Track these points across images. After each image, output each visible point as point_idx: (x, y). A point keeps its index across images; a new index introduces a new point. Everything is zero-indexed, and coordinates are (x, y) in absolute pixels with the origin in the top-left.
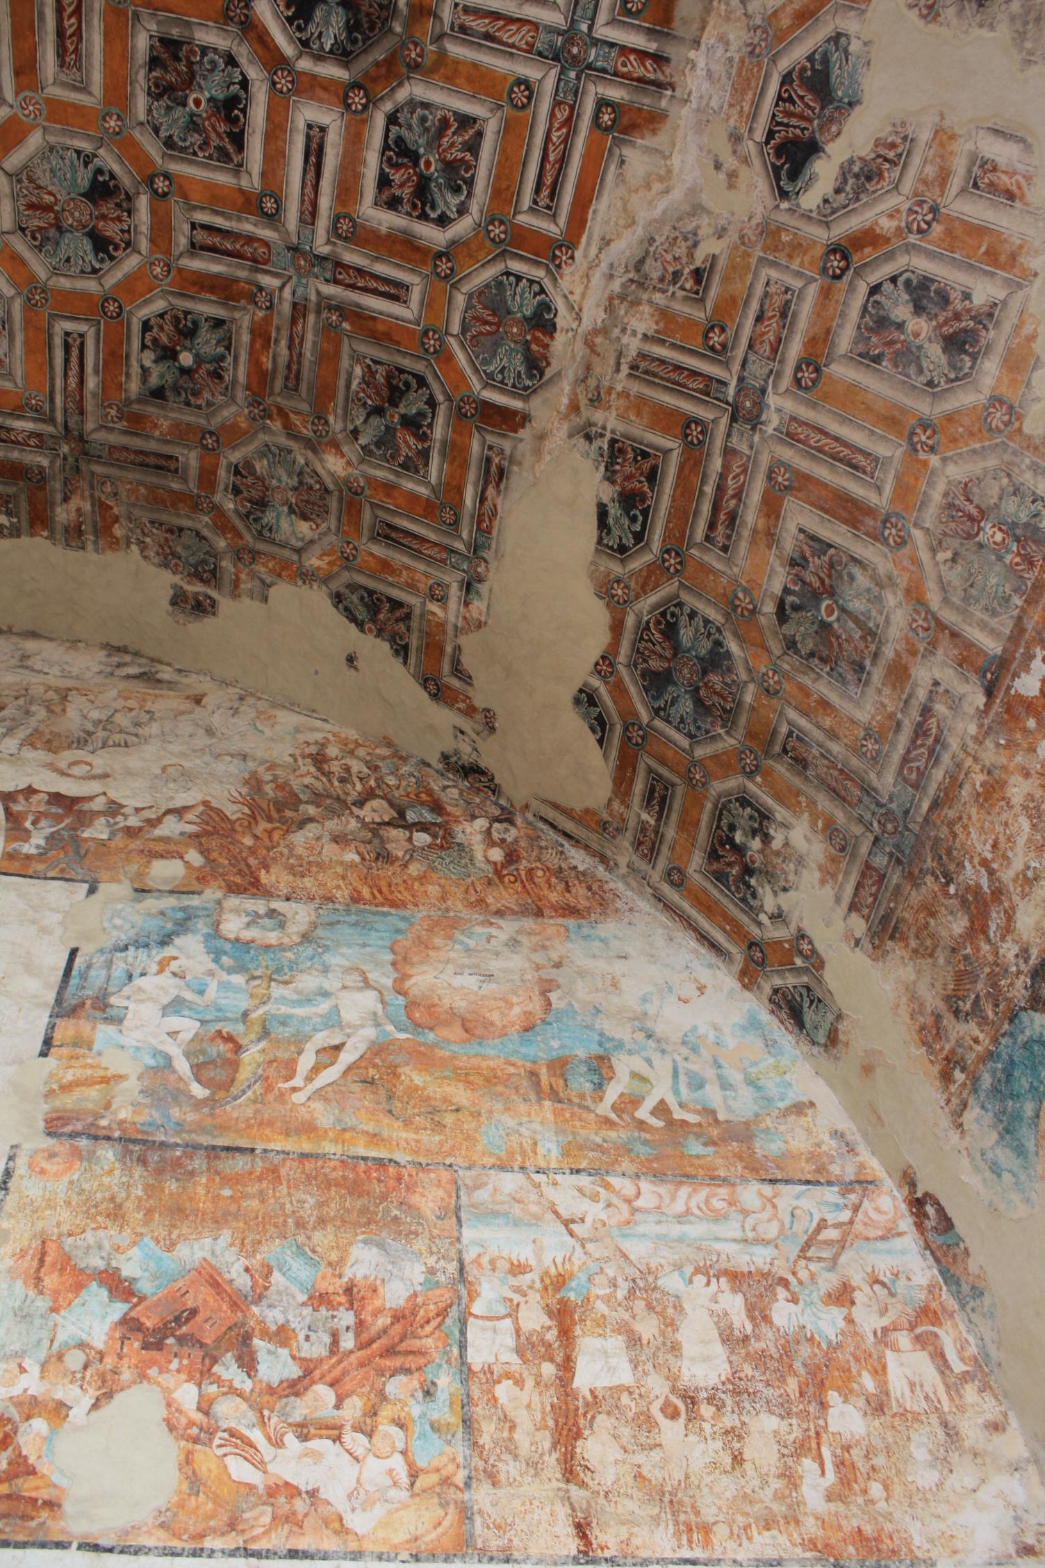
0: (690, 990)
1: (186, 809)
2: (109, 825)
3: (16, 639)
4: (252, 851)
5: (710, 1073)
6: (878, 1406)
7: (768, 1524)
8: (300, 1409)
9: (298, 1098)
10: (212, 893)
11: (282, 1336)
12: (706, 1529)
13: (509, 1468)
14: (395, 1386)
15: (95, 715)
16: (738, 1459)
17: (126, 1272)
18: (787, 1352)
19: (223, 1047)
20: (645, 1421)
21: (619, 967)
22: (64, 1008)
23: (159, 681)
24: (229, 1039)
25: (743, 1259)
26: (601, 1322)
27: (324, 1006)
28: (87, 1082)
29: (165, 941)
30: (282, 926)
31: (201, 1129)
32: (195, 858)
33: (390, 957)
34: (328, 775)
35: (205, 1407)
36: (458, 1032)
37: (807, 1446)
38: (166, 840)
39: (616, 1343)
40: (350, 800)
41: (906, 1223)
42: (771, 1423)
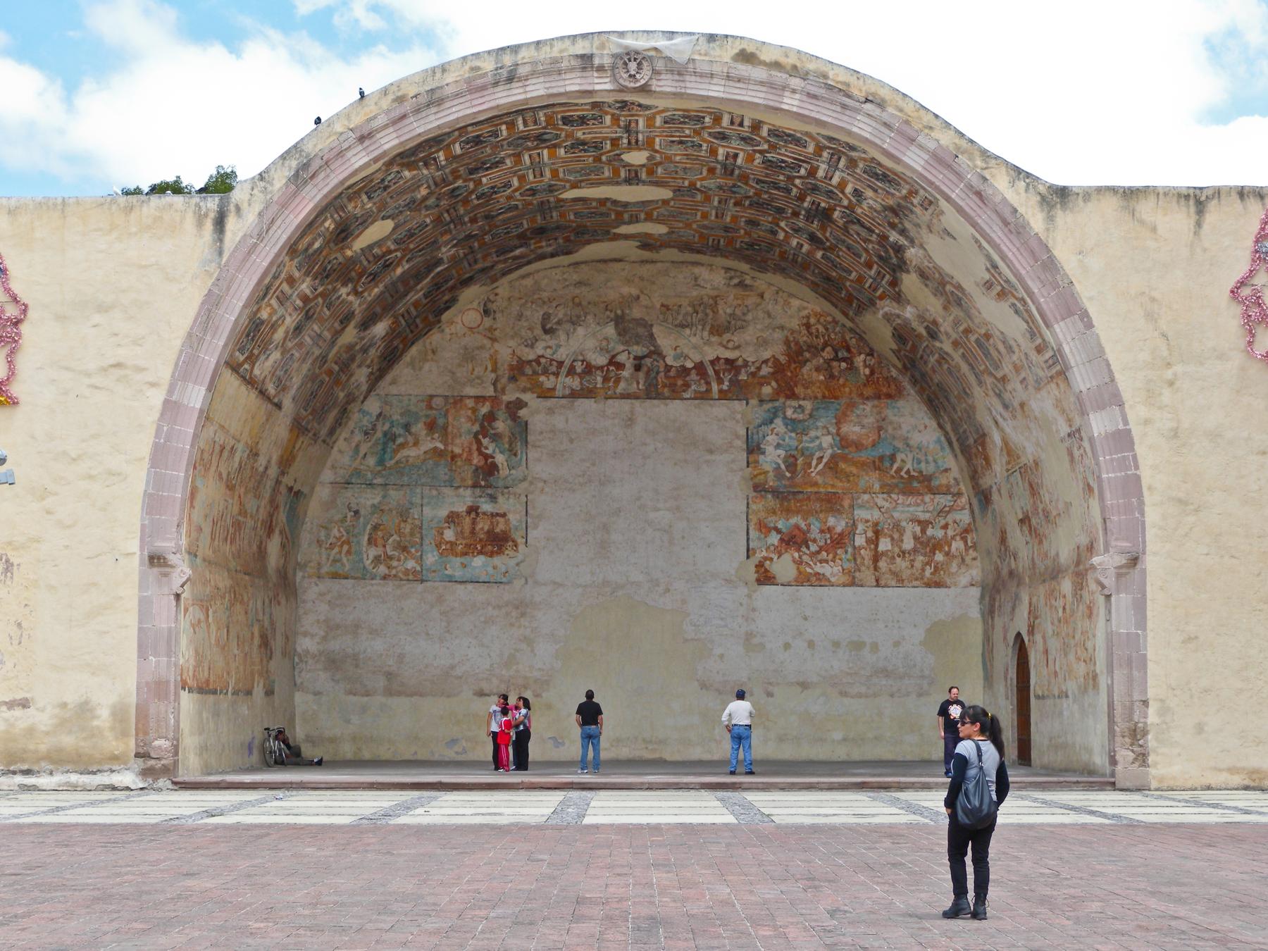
0: (922, 428)
1: (768, 360)
2: (746, 372)
3: (690, 267)
4: (791, 378)
5: (923, 458)
6: (947, 554)
7: (916, 579)
8: (820, 557)
9: (813, 474)
10: (782, 400)
11: (814, 541)
12: (903, 581)
13: (863, 568)
14: (839, 551)
15: (729, 311)
16: (912, 566)
17: (780, 526)
18: (929, 541)
19: (792, 460)
20: (893, 558)
21: (902, 420)
22: (750, 451)
23: (746, 286)
24: (794, 456)
25: (923, 516)
26: (885, 535)
27: (817, 442)
28: (760, 474)
29: (771, 422)
30: (803, 411)
31: (790, 486)
32: (774, 384)
33: (834, 421)
34: (811, 334)
35: (800, 557)
36: (853, 449)
37: (928, 563)
38: (763, 377)
39: (888, 540)
40: (820, 347)
41: (967, 506)
42: (921, 558)
